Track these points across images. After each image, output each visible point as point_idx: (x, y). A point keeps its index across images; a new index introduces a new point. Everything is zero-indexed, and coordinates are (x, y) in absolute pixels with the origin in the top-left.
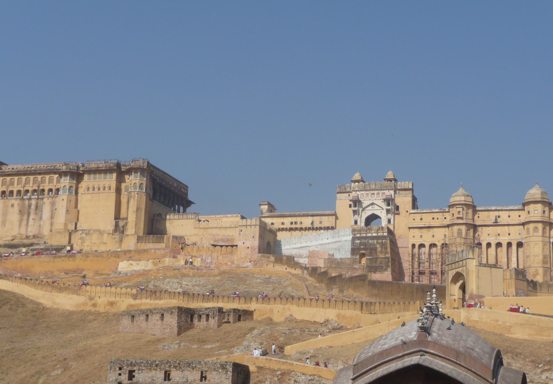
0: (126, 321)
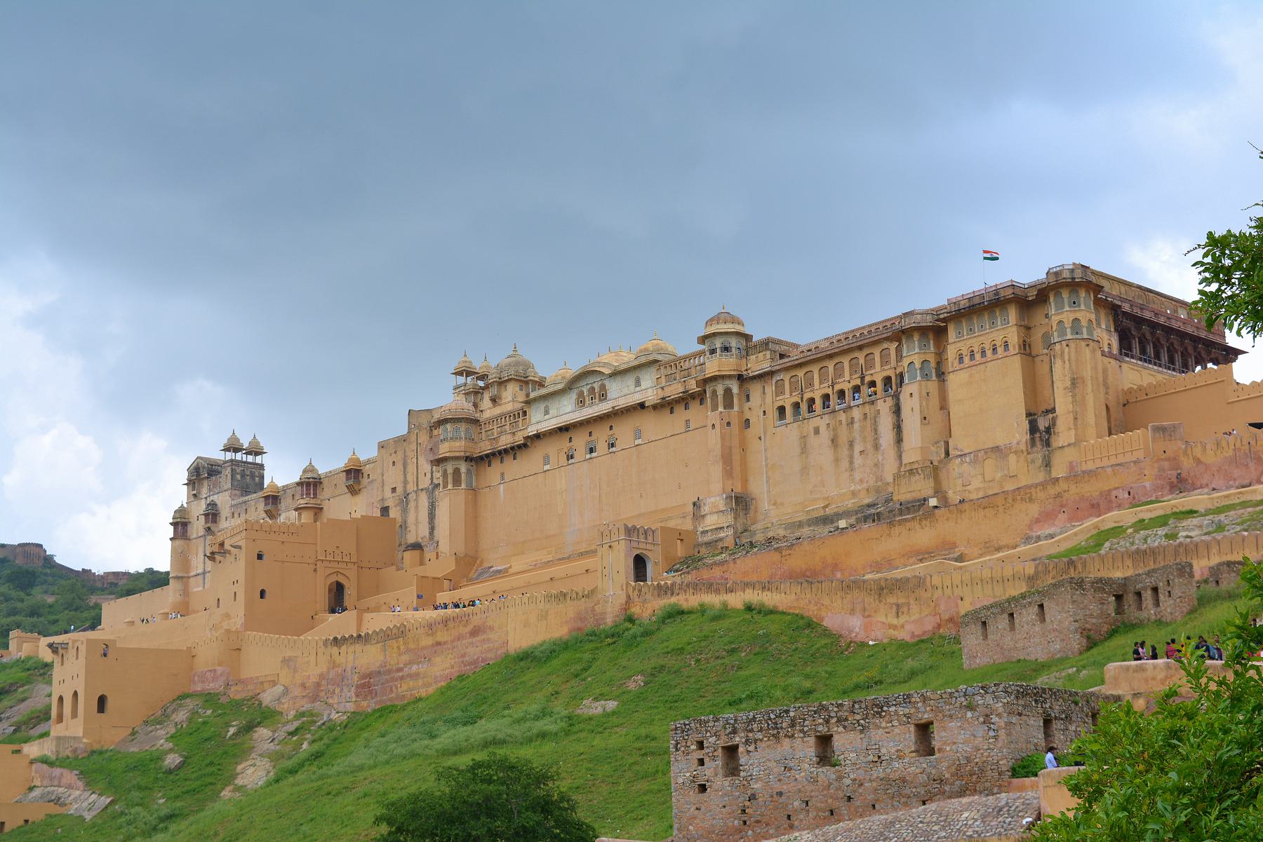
0: (971, 639)
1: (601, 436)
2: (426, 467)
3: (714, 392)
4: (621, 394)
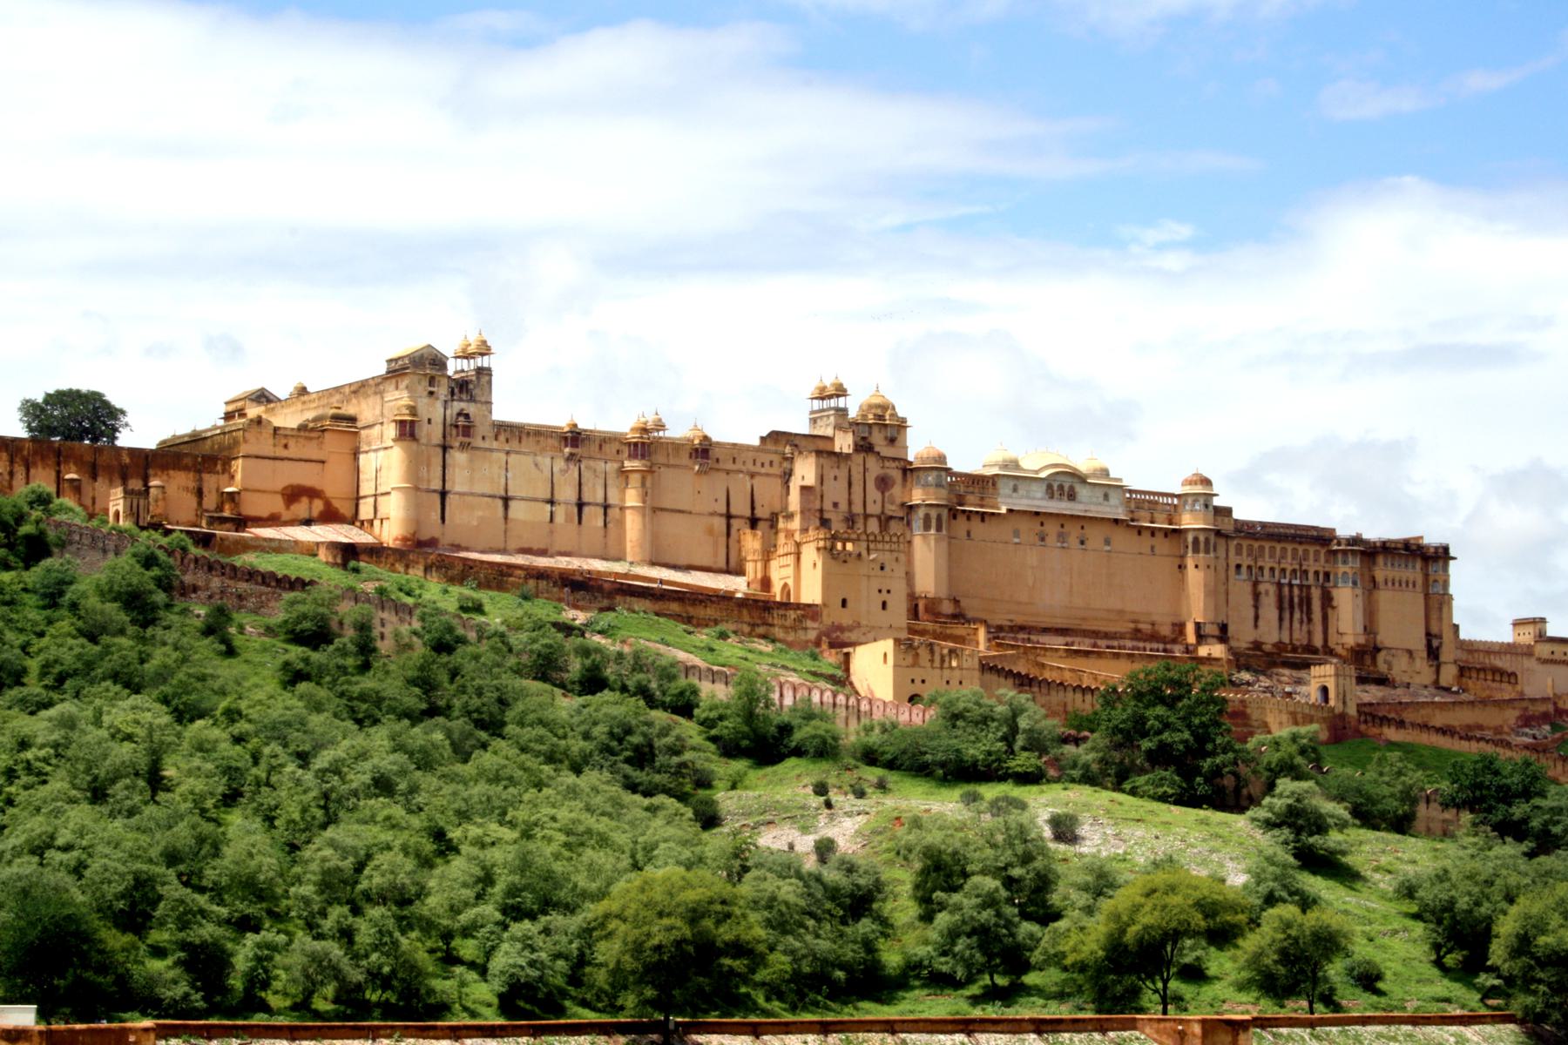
1: (1074, 532)
2: (873, 494)
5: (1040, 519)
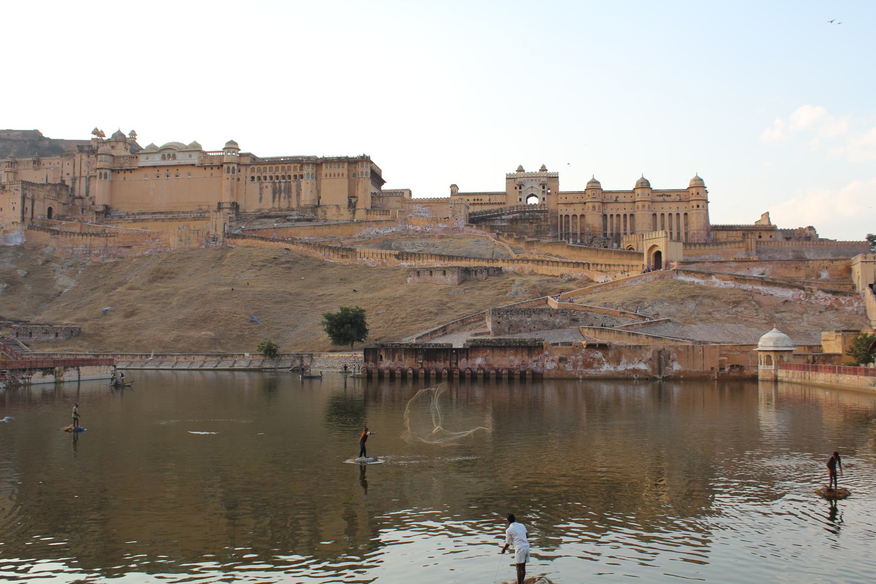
1: (173, 172)
3: (228, 168)
4: (182, 159)
5: (156, 170)
